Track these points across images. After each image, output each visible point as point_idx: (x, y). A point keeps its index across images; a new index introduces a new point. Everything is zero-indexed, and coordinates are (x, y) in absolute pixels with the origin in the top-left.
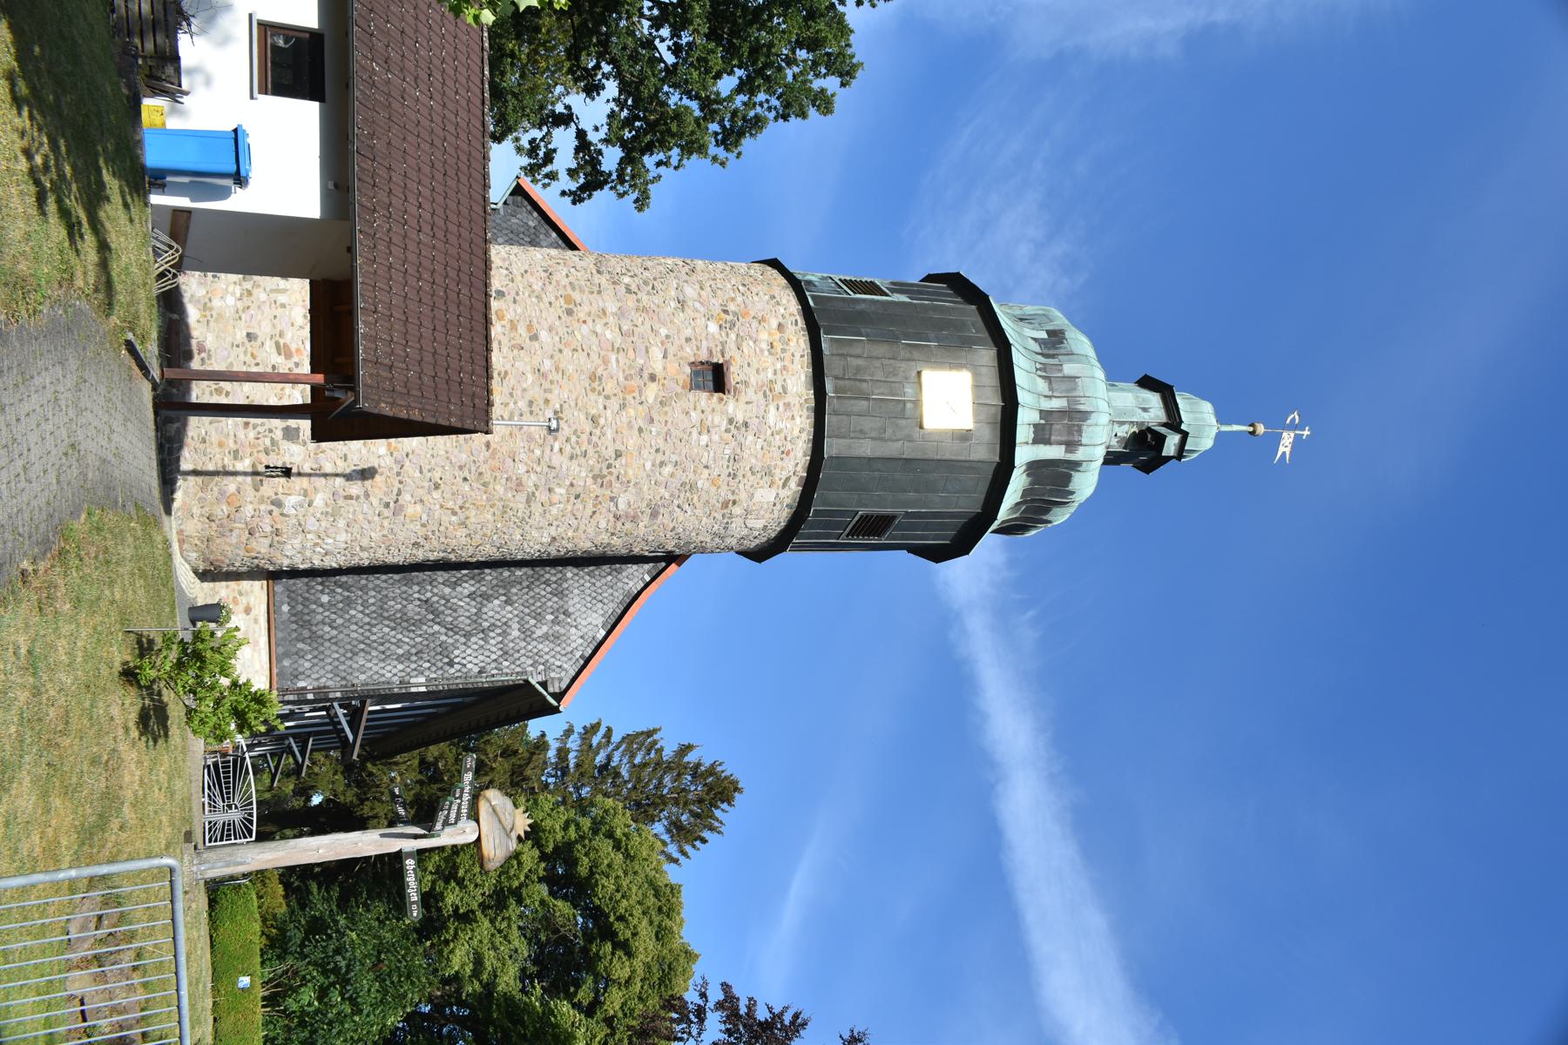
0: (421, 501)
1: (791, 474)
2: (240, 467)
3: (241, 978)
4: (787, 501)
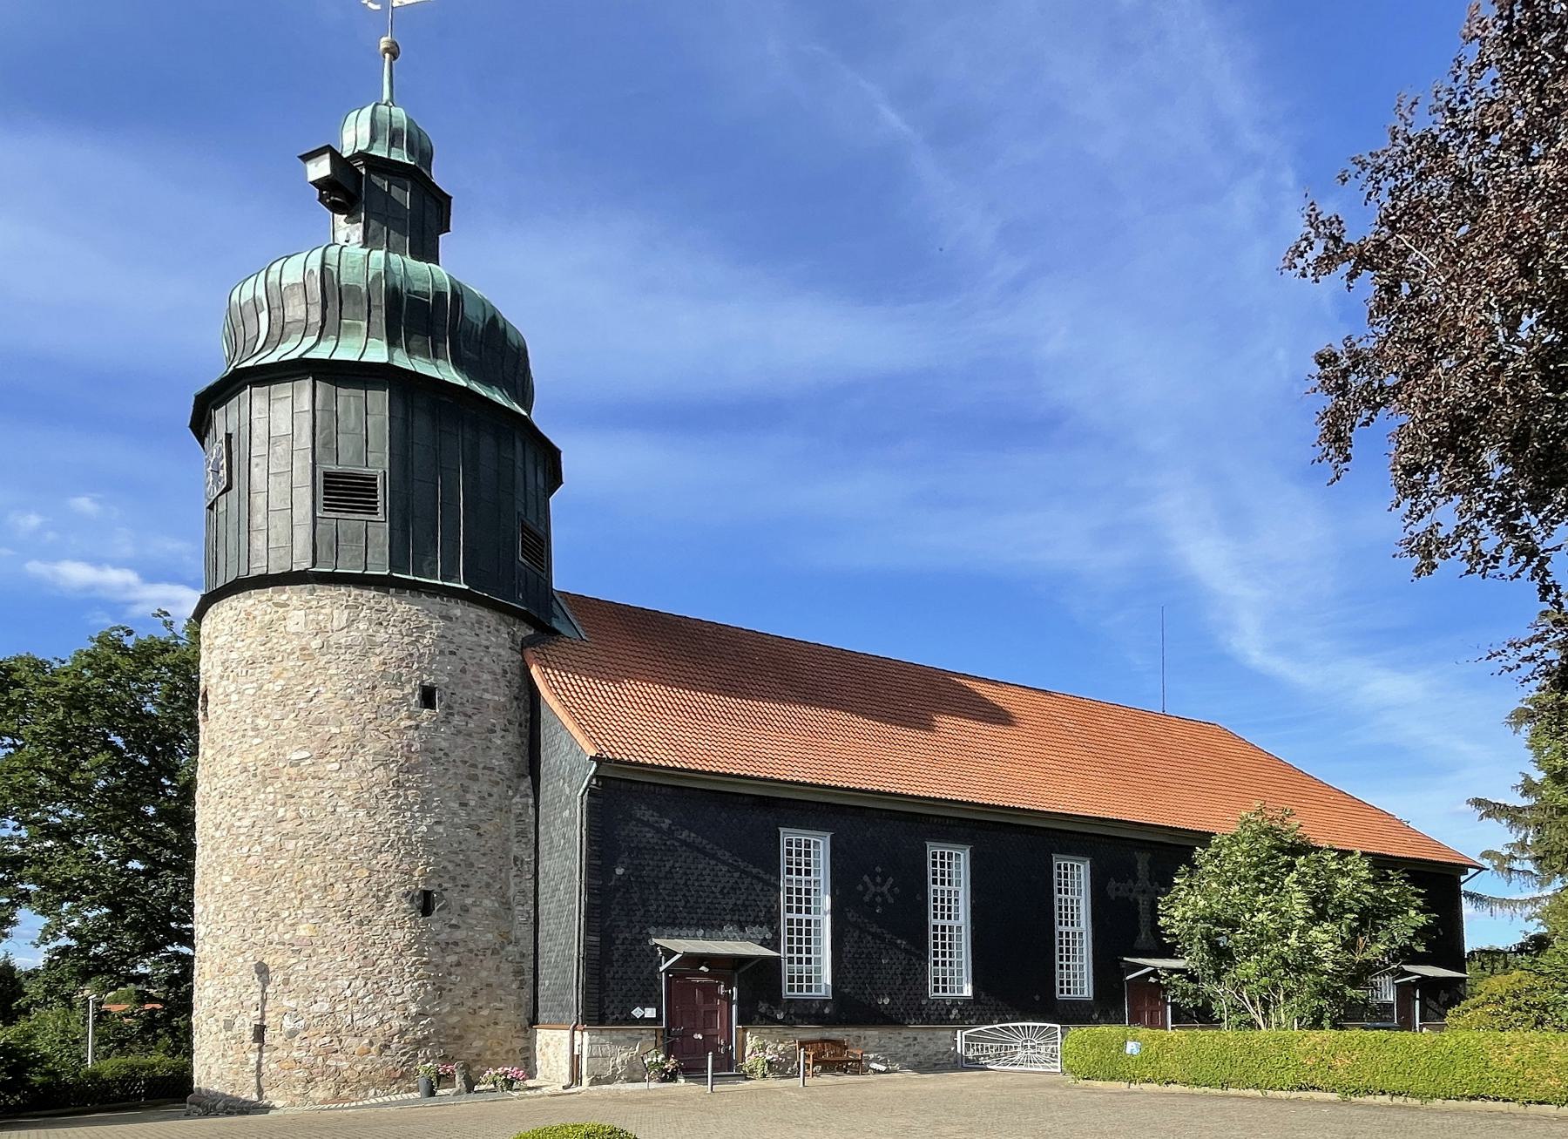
1: (270, 603)
2: (253, 1058)
3: (1128, 1051)
4: (306, 596)
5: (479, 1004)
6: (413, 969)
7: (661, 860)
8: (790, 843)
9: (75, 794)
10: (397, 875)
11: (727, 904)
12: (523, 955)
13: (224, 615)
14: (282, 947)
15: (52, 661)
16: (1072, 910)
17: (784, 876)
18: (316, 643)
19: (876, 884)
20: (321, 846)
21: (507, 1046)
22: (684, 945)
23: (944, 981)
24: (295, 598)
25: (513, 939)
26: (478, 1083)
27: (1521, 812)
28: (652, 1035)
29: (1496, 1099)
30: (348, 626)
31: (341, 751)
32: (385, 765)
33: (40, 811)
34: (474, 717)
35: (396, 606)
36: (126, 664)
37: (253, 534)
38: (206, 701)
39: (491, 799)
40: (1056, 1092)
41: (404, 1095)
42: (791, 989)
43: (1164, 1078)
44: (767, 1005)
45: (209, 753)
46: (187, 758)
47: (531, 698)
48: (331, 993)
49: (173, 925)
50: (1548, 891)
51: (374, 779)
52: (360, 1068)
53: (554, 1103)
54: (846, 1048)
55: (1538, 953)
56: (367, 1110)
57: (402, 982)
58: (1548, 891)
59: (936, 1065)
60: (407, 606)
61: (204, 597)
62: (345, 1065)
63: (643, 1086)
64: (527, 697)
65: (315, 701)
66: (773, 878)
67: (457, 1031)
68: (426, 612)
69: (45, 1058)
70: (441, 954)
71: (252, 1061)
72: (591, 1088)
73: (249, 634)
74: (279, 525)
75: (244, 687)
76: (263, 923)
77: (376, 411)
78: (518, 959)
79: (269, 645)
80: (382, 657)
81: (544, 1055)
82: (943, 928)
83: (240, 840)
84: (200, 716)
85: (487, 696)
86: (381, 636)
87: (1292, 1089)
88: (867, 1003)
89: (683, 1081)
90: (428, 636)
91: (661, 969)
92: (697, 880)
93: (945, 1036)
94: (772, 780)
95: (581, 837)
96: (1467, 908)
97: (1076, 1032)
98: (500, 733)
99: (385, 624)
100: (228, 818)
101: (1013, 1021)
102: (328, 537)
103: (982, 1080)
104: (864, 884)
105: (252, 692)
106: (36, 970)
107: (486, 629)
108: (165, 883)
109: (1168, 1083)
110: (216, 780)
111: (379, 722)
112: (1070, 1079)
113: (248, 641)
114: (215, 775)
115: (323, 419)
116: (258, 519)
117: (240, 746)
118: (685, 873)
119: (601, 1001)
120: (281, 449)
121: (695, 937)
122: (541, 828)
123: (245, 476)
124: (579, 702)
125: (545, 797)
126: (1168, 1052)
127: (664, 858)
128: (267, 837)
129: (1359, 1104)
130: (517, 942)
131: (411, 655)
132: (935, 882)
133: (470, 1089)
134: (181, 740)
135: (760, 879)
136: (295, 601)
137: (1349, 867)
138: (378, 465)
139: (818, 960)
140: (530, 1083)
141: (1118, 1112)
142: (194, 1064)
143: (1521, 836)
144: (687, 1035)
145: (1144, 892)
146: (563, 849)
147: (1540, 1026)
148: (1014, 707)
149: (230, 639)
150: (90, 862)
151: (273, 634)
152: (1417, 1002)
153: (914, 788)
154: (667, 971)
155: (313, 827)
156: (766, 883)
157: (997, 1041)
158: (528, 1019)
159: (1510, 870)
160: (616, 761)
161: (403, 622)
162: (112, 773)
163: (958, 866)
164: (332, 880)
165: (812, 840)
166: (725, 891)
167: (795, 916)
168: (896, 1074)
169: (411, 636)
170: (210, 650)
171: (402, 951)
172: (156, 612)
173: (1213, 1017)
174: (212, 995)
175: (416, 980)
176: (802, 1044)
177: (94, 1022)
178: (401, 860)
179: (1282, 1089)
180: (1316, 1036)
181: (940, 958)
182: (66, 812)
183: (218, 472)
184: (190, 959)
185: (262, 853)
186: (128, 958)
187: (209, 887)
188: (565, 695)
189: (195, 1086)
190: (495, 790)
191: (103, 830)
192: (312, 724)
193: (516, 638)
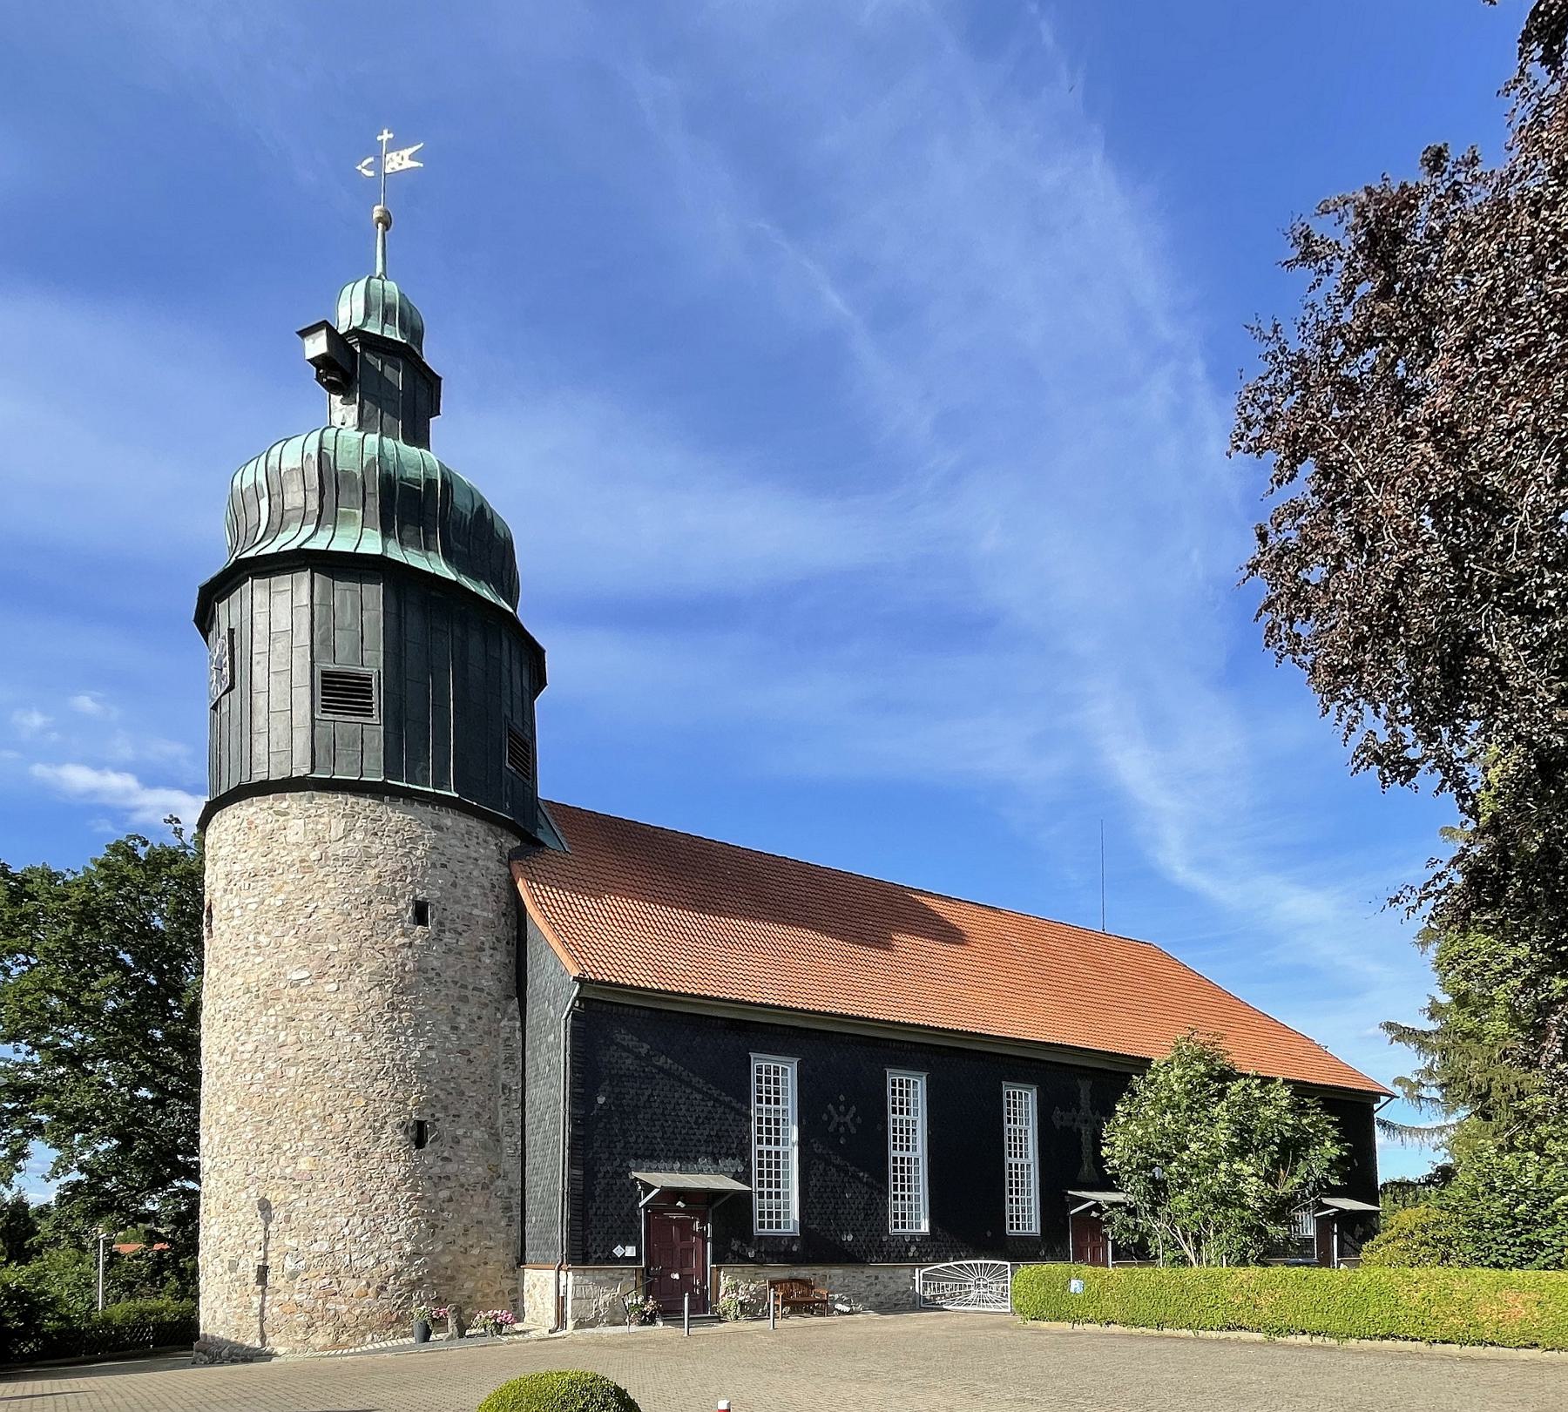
1: (271, 812)
2: (257, 1300)
3: (1072, 1290)
4: (305, 804)
5: (470, 1243)
6: (408, 1205)
7: (640, 1088)
8: (759, 1070)
9: (85, 1014)
10: (393, 1104)
11: (702, 1134)
12: (511, 1190)
13: (227, 824)
14: (283, 1182)
15: (64, 872)
16: (1021, 1141)
17: (754, 1104)
18: (314, 855)
19: (839, 1113)
20: (320, 1074)
21: (497, 1287)
22: (662, 1179)
23: (903, 1216)
24: (295, 805)
25: (501, 1172)
26: (469, 1327)
27: (1427, 1037)
28: (632, 1275)
29: (1406, 1339)
30: (345, 837)
31: (339, 970)
32: (380, 985)
33: (52, 1034)
34: (465, 934)
35: (391, 815)
36: (138, 875)
37: (255, 737)
38: (210, 916)
39: (482, 1022)
40: (1006, 1333)
41: (400, 1340)
42: (762, 1225)
43: (1105, 1319)
44: (739, 1243)
45: (214, 972)
46: (193, 977)
47: (517, 913)
48: (331, 1231)
49: (180, 1157)
50: (1453, 1120)
51: (370, 1001)
52: (358, 1312)
53: (540, 1348)
54: (813, 1288)
55: (1444, 1185)
56: (365, 1358)
57: (398, 1219)
58: (1453, 1120)
59: (896, 1305)
60: (401, 815)
61: (208, 804)
62: (344, 1308)
63: (625, 1328)
64: (514, 912)
65: (314, 917)
66: (744, 1107)
67: (449, 1272)
68: (419, 822)
69: (56, 1300)
70: (434, 1189)
71: (256, 1305)
72: (575, 1332)
73: (251, 845)
74: (279, 726)
75: (247, 901)
76: (265, 1156)
77: (370, 606)
78: (506, 1194)
79: (270, 856)
80: (377, 870)
81: (531, 1296)
82: (902, 1160)
83: (244, 1066)
84: (205, 933)
85: (476, 912)
86: (376, 848)
87: (1221, 1329)
88: (831, 1239)
89: (661, 1323)
90: (421, 847)
91: (641, 1205)
92: (674, 1109)
93: (905, 1275)
94: (743, 1002)
95: (566, 1064)
96: (1380, 1137)
97: (1027, 1270)
98: (488, 952)
99: (380, 834)
100: (232, 1043)
101: (967, 1258)
102: (327, 740)
103: (937, 1321)
104: (829, 1113)
105: (254, 906)
106: (47, 1206)
107: (475, 840)
108: (173, 1112)
109: (1108, 1323)
110: (220, 1001)
111: (374, 939)
112: (1019, 1319)
113: (251, 852)
114: (219, 996)
115: (320, 611)
116: (260, 721)
117: (243, 965)
118: (662, 1102)
119: (584, 1239)
120: (281, 646)
121: (672, 1170)
122: (528, 1054)
123: (247, 673)
124: (563, 919)
125: (531, 1021)
126: (1108, 1291)
127: (643, 1086)
128: (269, 1063)
129: (1283, 1345)
130: (505, 1177)
131: (405, 867)
132: (894, 1111)
133: (461, 1335)
134: (187, 958)
135: (733, 1108)
136: (295, 810)
137: (1272, 1095)
138: (373, 664)
139: (787, 1195)
140: (518, 1326)
141: (1064, 1354)
142: (200, 1309)
143: (1428, 1062)
144: (664, 1275)
145: (1086, 1121)
146: (548, 1077)
147: (1445, 1262)
148: (966, 925)
149: (234, 850)
150: (101, 1091)
151: (274, 844)
152: (1335, 1237)
153: (875, 1011)
154: (646, 1207)
155: (313, 1052)
156: (738, 1112)
157: (953, 1280)
158: (516, 1258)
159: (1420, 1097)
160: (598, 982)
161: (397, 832)
162: (121, 994)
163: (916, 1094)
164: (331, 1110)
165: (781, 1066)
166: (700, 1121)
167: (765, 1147)
168: (859, 1316)
169: (404, 847)
170: (214, 861)
171: (397, 1186)
172: (168, 818)
173: (1149, 1253)
174: (217, 1234)
175: (411, 1217)
176: (773, 1284)
177: (105, 1263)
178: (396, 1088)
179: (1212, 1329)
180: (1242, 1273)
181: (899, 1193)
182: (78, 1035)
183: (221, 670)
184: (196, 1194)
185: (265, 1080)
186: (136, 1194)
187: (214, 1117)
188: (550, 911)
189: (201, 1332)
190: (484, 1012)
191: (112, 1056)
192: (311, 941)
193: (503, 850)
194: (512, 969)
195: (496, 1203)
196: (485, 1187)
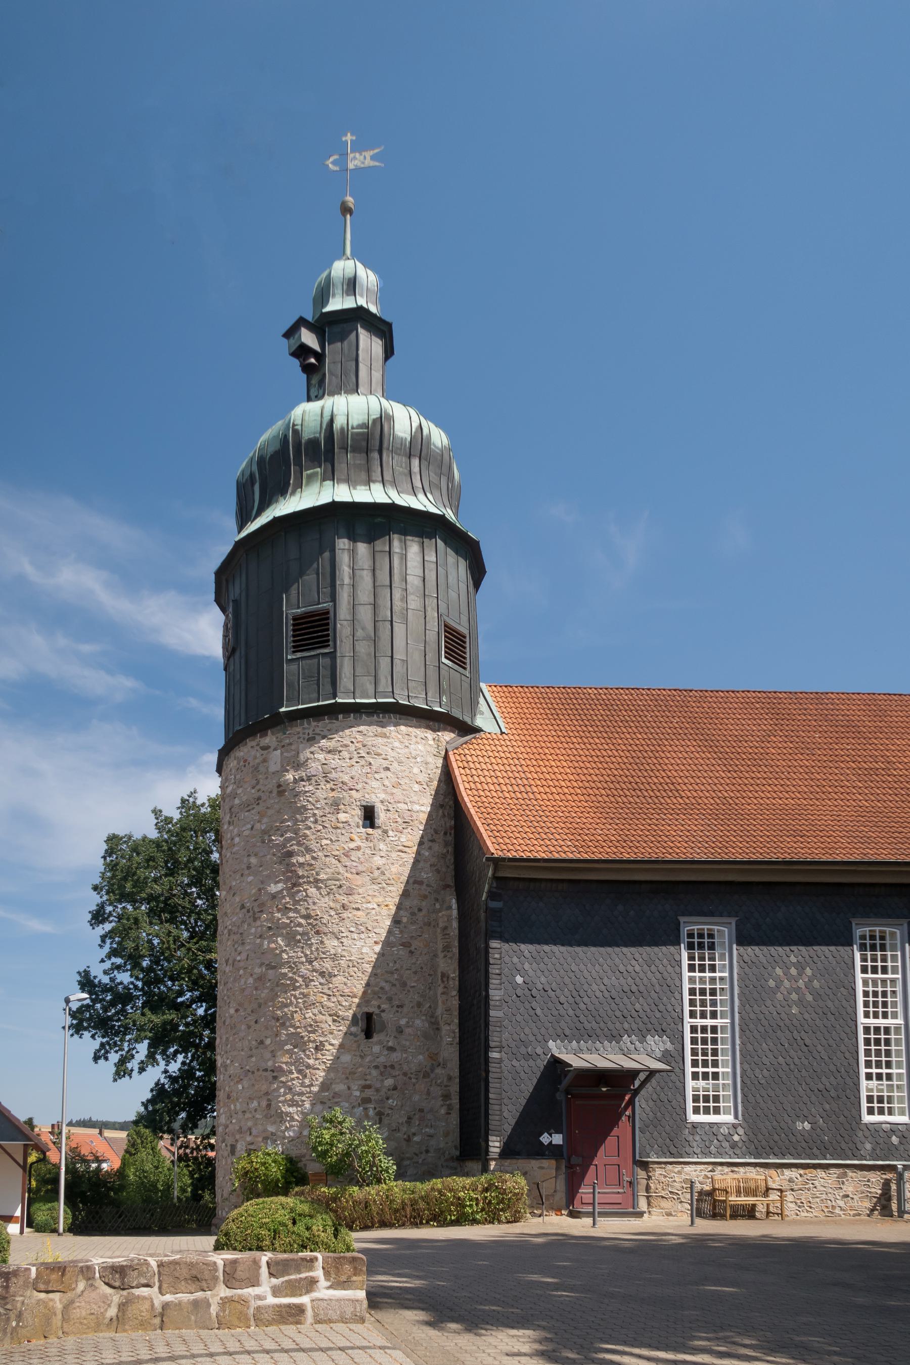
0: (272, 1051)
12: (450, 1078)
25: (441, 1060)
39: (421, 914)
78: (445, 1083)
167: (699, 1022)
190: (424, 903)
194: (450, 858)
195: (437, 1091)
196: (426, 1075)
